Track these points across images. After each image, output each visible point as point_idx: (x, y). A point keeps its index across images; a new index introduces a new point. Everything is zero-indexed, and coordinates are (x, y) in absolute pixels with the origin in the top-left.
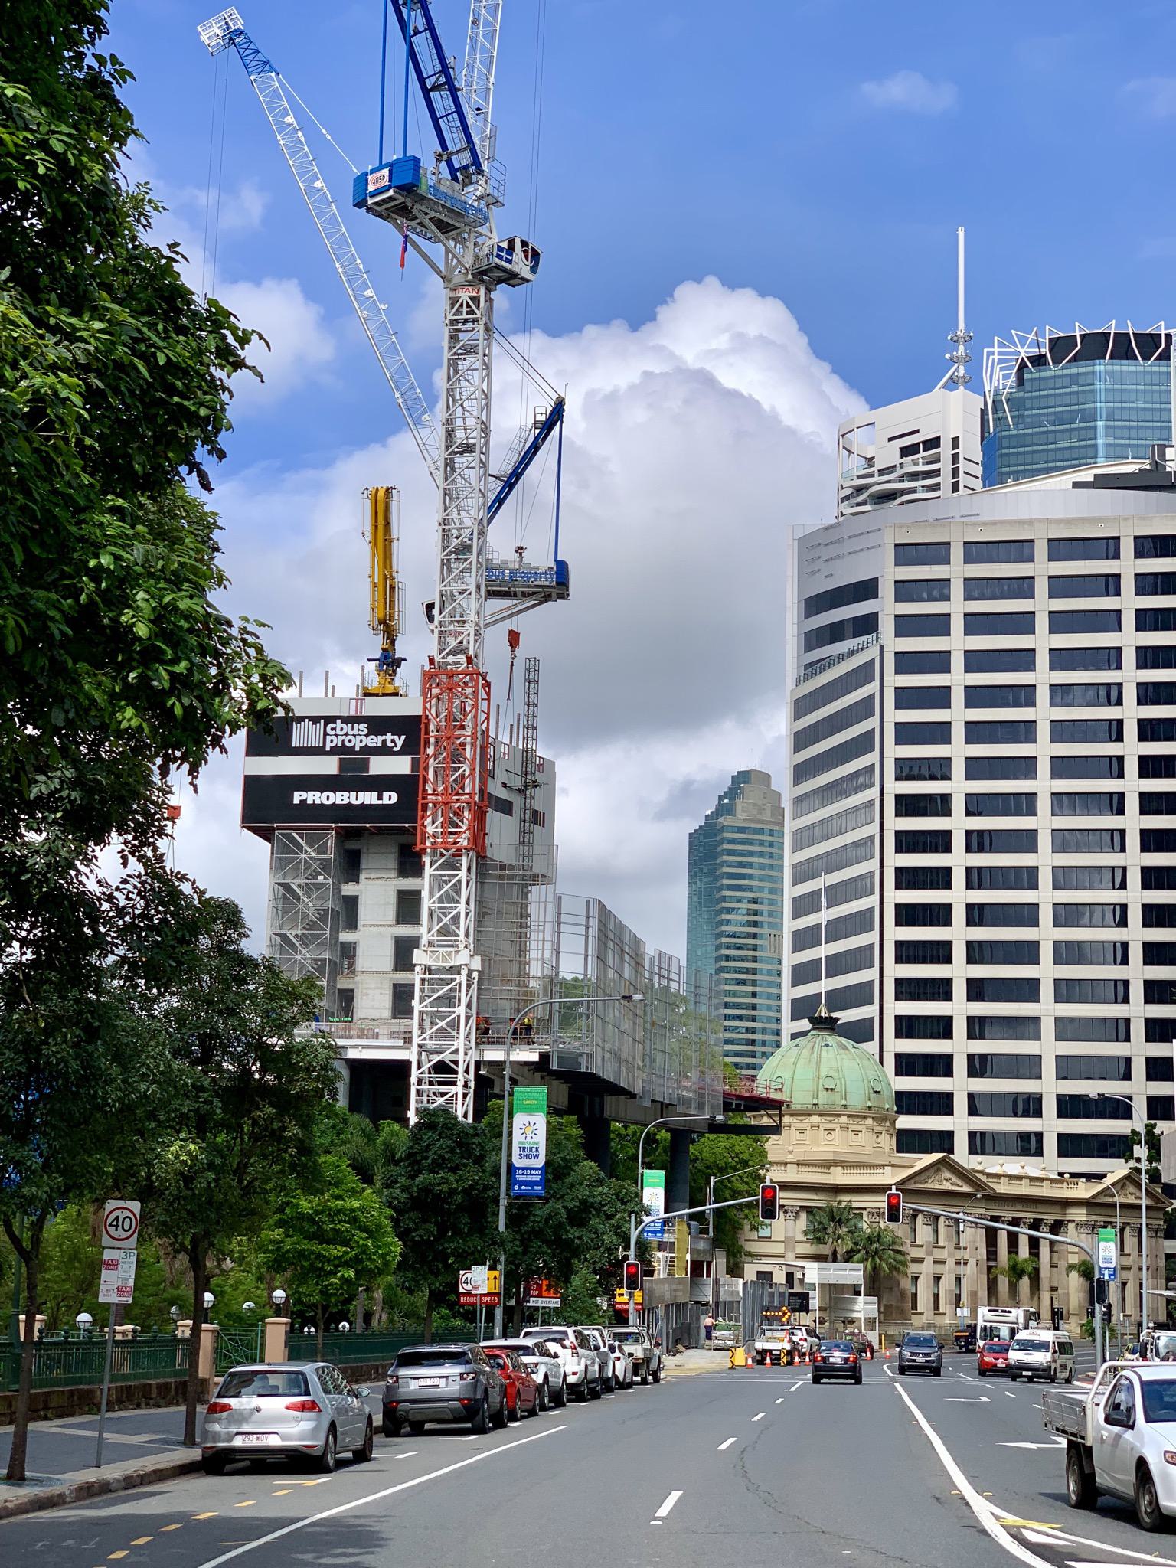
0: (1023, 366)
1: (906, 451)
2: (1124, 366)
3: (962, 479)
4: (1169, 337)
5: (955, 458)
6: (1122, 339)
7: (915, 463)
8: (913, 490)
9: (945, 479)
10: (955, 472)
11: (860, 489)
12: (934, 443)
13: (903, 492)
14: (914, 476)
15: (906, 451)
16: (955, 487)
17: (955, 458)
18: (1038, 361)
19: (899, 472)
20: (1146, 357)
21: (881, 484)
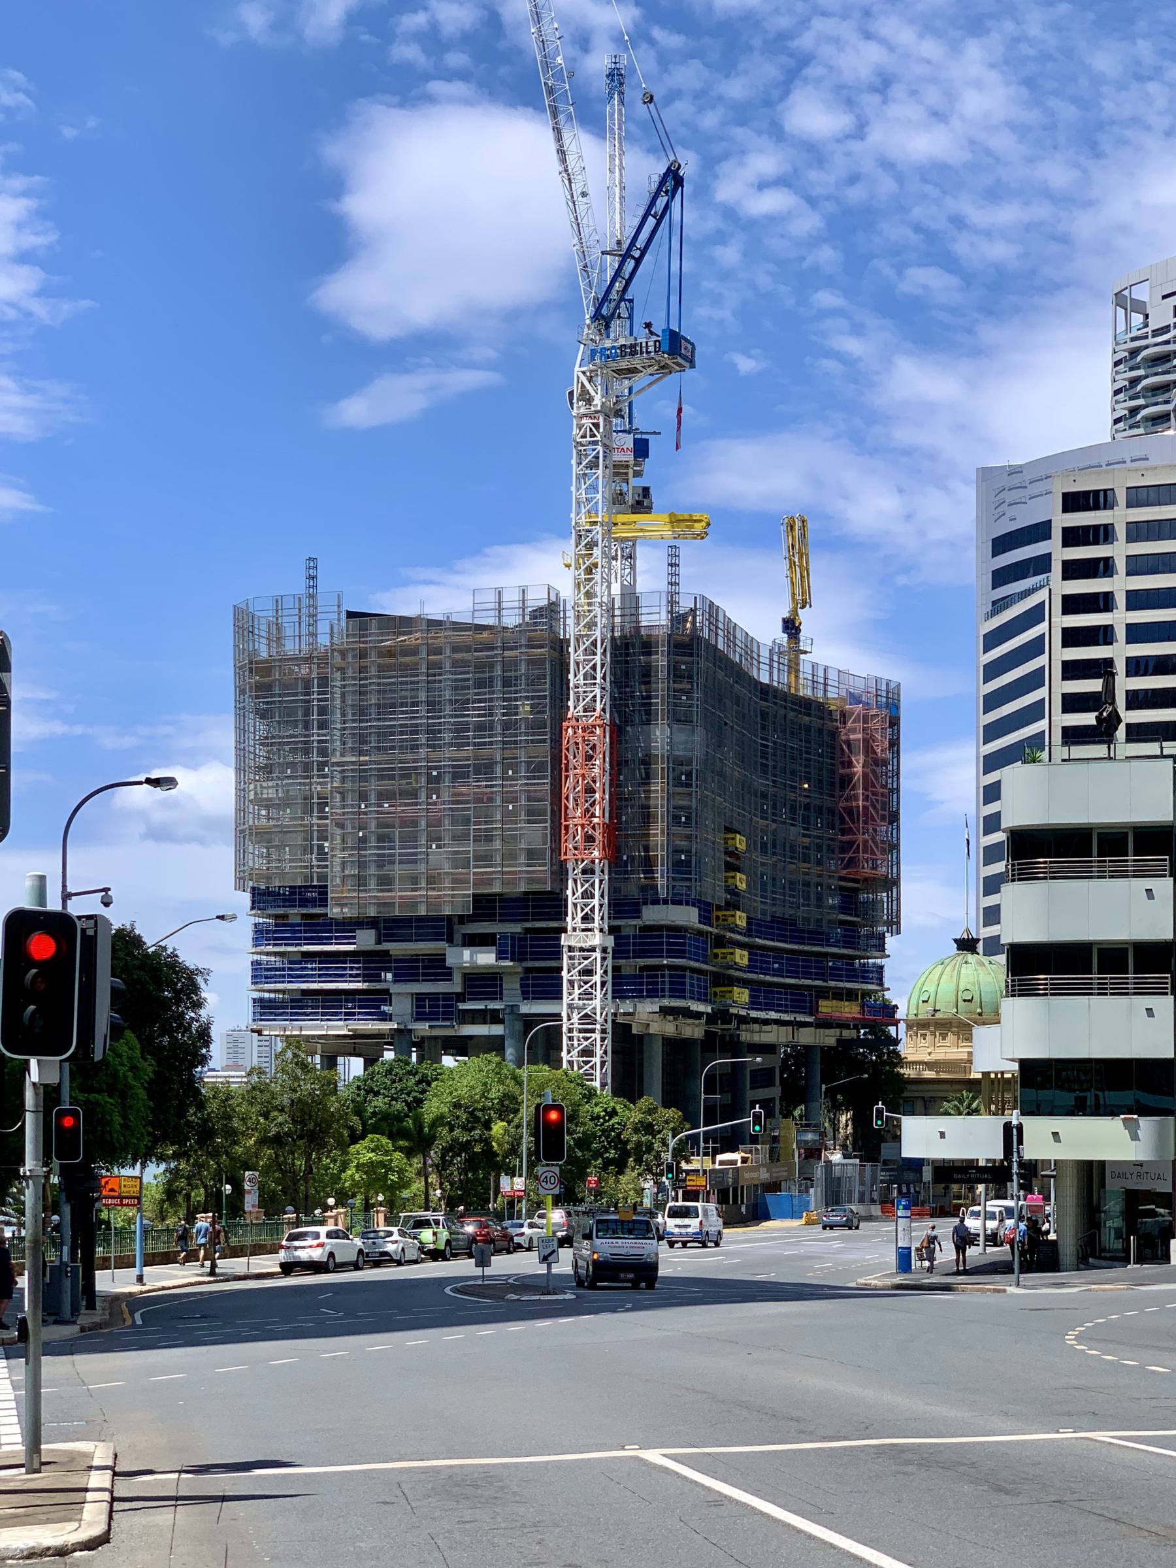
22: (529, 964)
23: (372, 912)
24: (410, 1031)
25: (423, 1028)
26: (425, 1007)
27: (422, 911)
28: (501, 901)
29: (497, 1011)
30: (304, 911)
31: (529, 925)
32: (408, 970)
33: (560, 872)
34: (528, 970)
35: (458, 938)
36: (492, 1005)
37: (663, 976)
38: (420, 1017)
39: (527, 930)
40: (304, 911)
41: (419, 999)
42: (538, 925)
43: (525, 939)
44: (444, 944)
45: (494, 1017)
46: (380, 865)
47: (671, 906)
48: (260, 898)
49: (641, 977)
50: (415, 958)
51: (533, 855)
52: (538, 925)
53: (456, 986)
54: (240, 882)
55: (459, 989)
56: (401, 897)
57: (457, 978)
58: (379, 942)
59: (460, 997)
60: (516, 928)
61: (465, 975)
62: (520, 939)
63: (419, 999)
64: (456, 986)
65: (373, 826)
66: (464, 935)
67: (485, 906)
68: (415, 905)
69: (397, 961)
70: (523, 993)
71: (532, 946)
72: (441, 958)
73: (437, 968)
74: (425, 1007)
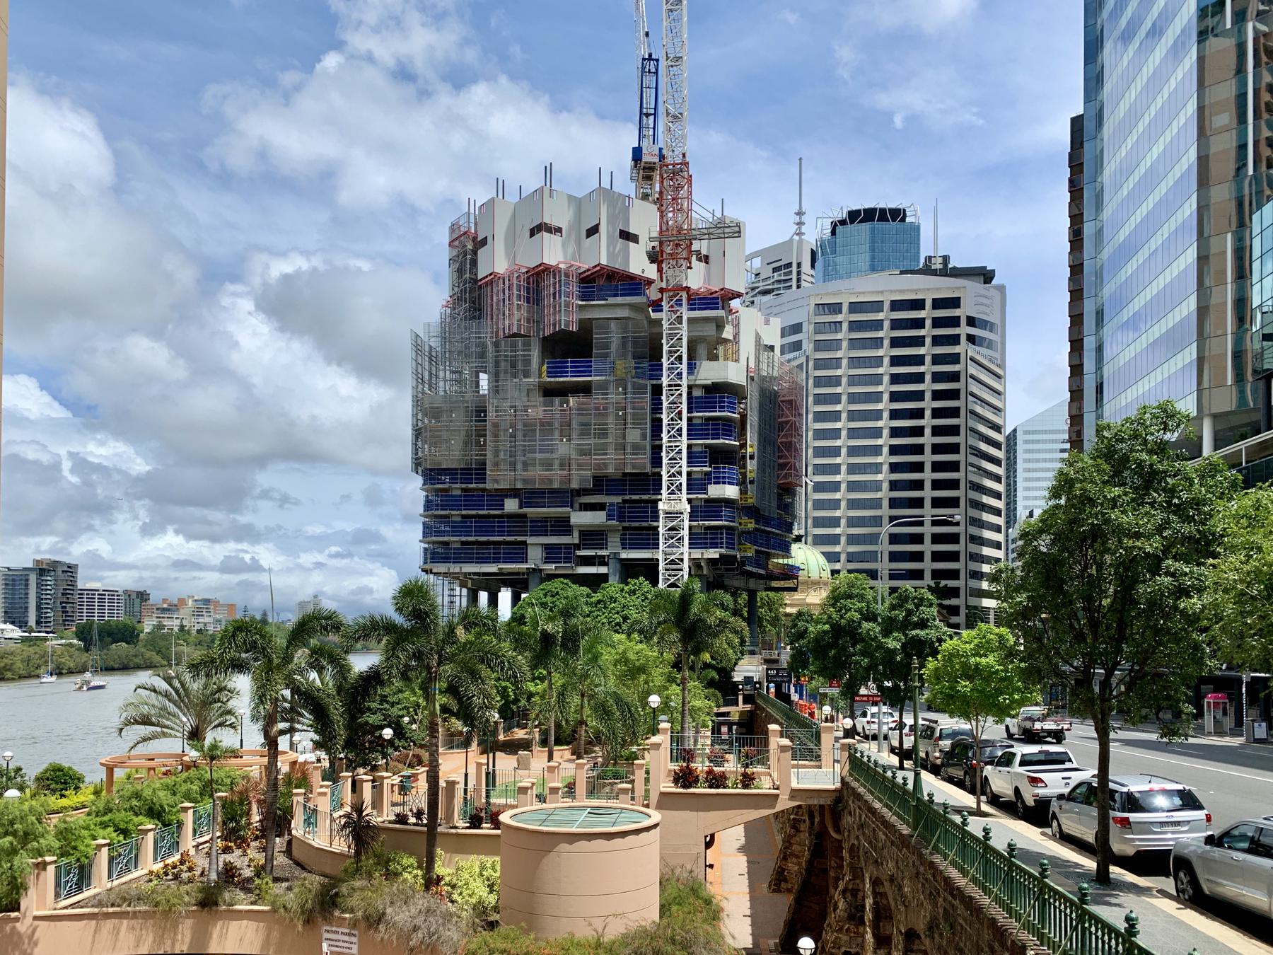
0: (836, 225)
1: (775, 270)
2: (883, 225)
3: (803, 284)
4: (904, 210)
5: (799, 273)
6: (883, 211)
7: (780, 275)
8: (779, 289)
9: (794, 283)
10: (799, 280)
11: (753, 289)
12: (790, 265)
13: (773, 290)
14: (779, 281)
15: (775, 270)
16: (799, 287)
17: (799, 273)
18: (843, 222)
19: (772, 280)
20: (894, 220)
21: (762, 286)
22: (626, 524)
23: (519, 486)
24: (541, 570)
25: (551, 567)
26: (551, 553)
27: (556, 486)
28: (607, 481)
29: (604, 556)
30: (464, 486)
31: (627, 497)
32: (541, 527)
33: (657, 461)
34: (625, 528)
35: (577, 506)
36: (600, 553)
37: (722, 534)
38: (547, 560)
39: (624, 501)
40: (464, 486)
41: (548, 548)
42: (634, 497)
43: (624, 507)
44: (569, 509)
45: (602, 561)
46: (524, 453)
47: (727, 486)
48: (431, 475)
49: (706, 534)
50: (545, 520)
51: (637, 448)
52: (634, 497)
53: (574, 539)
54: (417, 463)
55: (576, 541)
56: (540, 475)
57: (576, 534)
58: (521, 507)
59: (578, 547)
60: (617, 499)
61: (580, 531)
62: (620, 507)
63: (548, 548)
64: (574, 539)
65: (520, 426)
66: (580, 504)
67: (601, 483)
68: (551, 481)
69: (531, 522)
70: (622, 544)
71: (629, 512)
72: (567, 519)
73: (563, 526)
74: (551, 553)
